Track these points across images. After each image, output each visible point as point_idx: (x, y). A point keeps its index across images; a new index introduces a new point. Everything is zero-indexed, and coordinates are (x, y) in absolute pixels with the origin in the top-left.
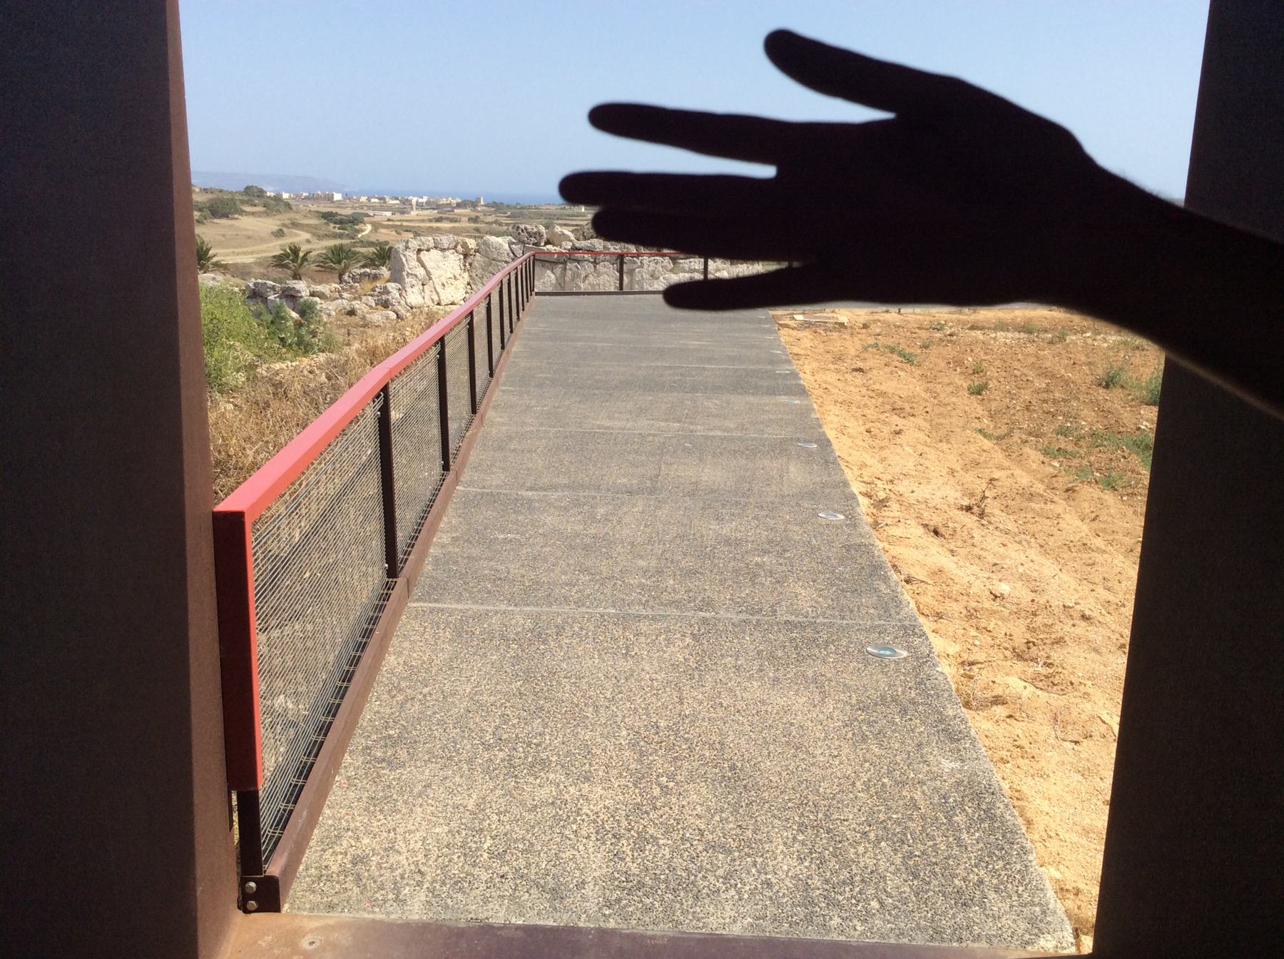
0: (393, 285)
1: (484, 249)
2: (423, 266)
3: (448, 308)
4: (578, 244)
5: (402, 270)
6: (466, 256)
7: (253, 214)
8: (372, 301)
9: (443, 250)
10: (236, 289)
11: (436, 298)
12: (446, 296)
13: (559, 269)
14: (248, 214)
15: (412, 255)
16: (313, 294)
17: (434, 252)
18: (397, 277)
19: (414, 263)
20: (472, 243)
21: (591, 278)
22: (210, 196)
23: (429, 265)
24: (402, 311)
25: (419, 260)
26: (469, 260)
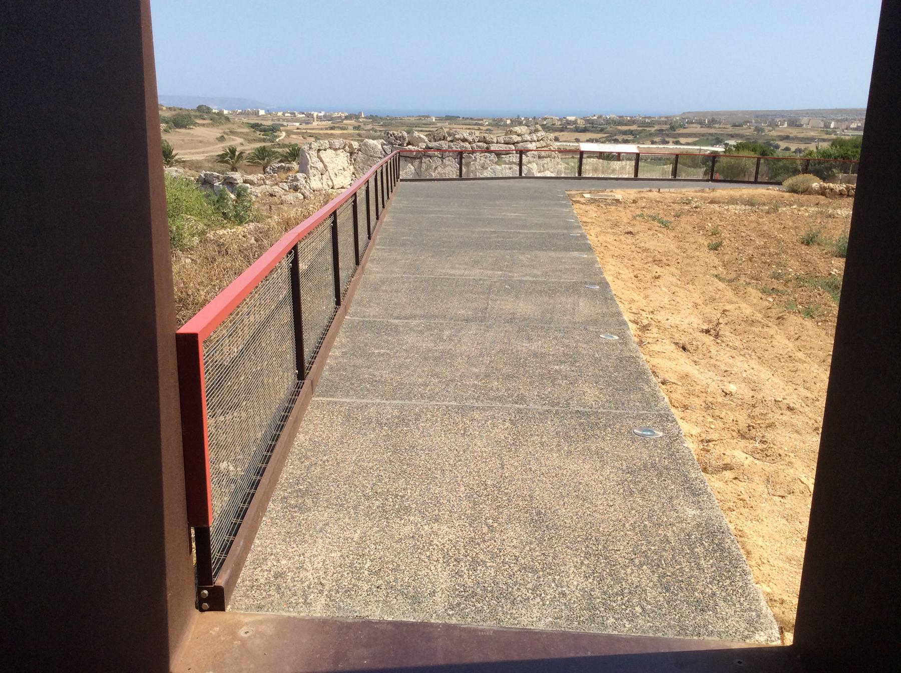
0: (301, 174)
1: (364, 148)
2: (322, 161)
3: (339, 191)
4: (430, 145)
5: (307, 163)
6: (351, 154)
7: (203, 125)
8: (286, 186)
9: (336, 150)
11: (330, 184)
12: (338, 182)
13: (417, 162)
14: (199, 125)
15: (314, 153)
16: (245, 182)
17: (329, 151)
18: (303, 169)
19: (315, 159)
20: (356, 145)
21: (439, 169)
22: (174, 113)
23: (326, 160)
24: (307, 193)
25: (319, 157)
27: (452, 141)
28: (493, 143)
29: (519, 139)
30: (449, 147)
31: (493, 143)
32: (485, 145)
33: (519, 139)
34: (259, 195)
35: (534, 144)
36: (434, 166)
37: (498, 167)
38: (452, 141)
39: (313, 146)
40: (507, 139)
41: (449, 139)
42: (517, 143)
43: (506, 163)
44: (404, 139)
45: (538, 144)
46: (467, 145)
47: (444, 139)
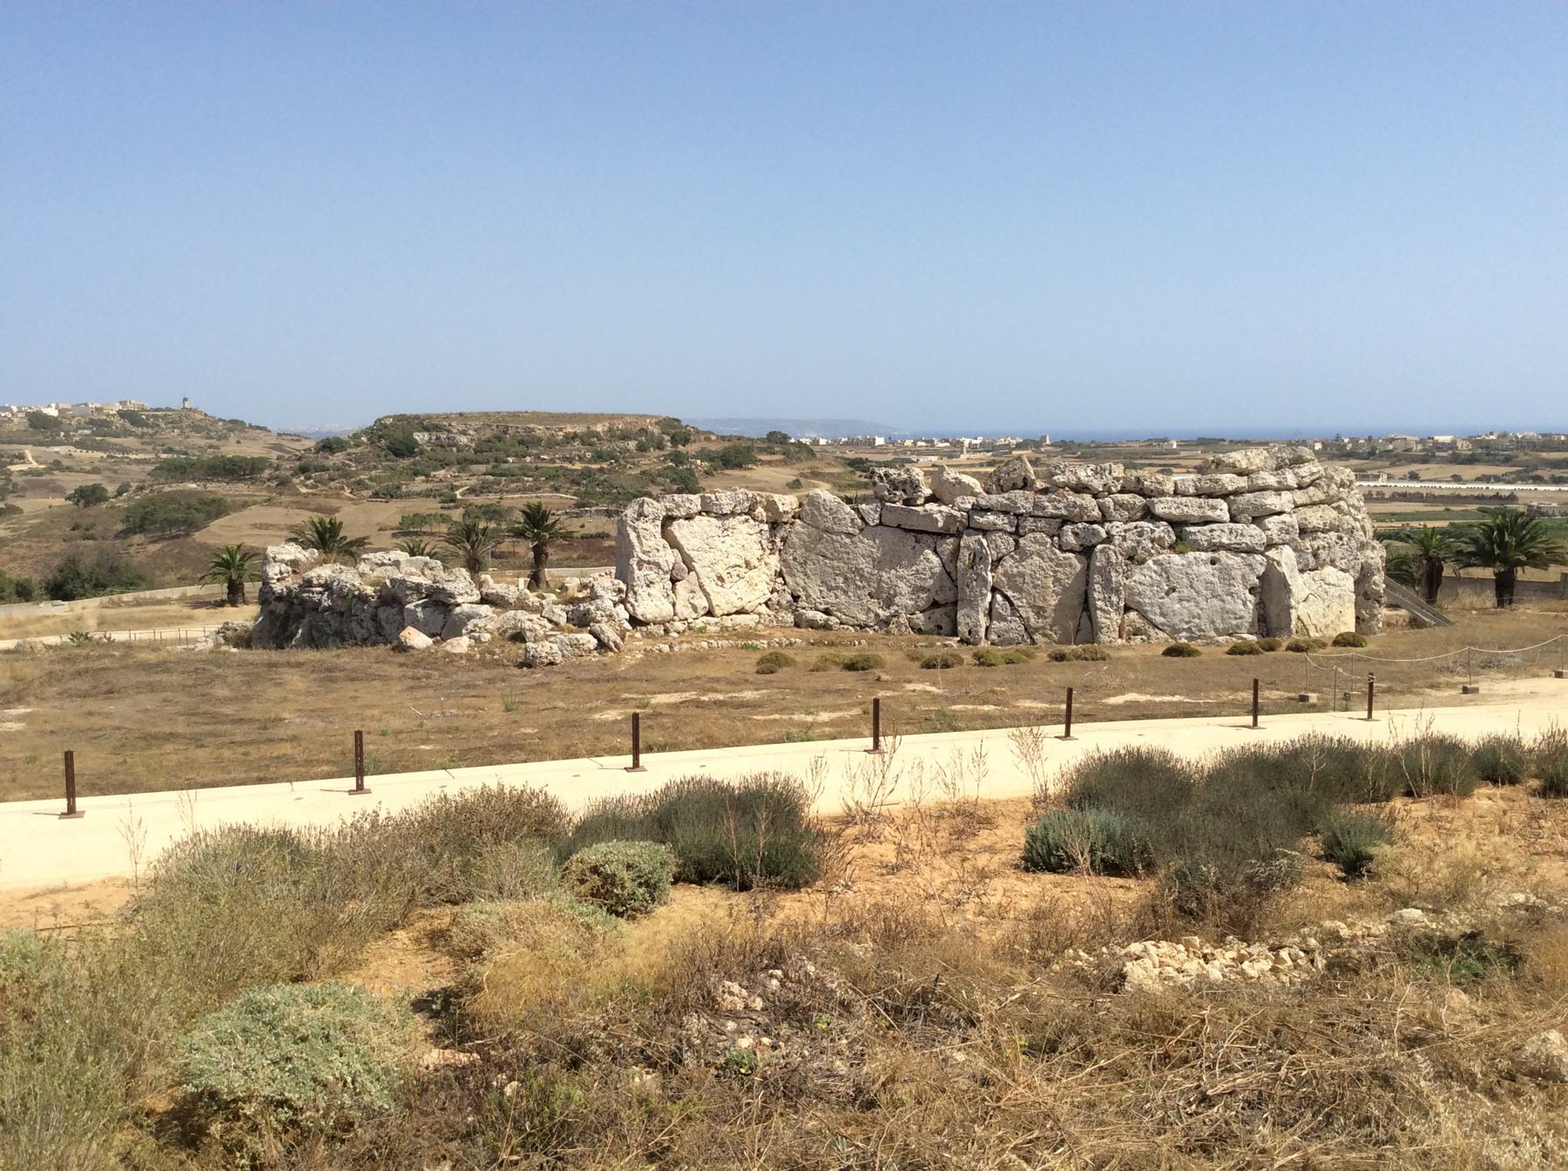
1: (808, 511)
2: (674, 544)
3: (728, 622)
4: (983, 503)
5: (630, 555)
6: (774, 525)
7: (770, 463)
9: (722, 516)
10: (369, 590)
12: (724, 599)
13: (948, 545)
14: (763, 463)
17: (702, 522)
20: (787, 503)
21: (1008, 563)
22: (727, 444)
24: (610, 634)
25: (666, 533)
26: (782, 533)
27: (1045, 491)
28: (1163, 494)
29: (1242, 482)
30: (1036, 505)
31: (1163, 494)
32: (1139, 501)
33: (1242, 482)
34: (486, 637)
35: (1286, 496)
36: (992, 555)
37: (1176, 558)
38: (1045, 491)
39: (647, 509)
40: (1206, 485)
41: (1039, 484)
42: (1237, 493)
43: (1198, 548)
44: (915, 487)
45: (1300, 497)
46: (1087, 500)
47: (1026, 484)
